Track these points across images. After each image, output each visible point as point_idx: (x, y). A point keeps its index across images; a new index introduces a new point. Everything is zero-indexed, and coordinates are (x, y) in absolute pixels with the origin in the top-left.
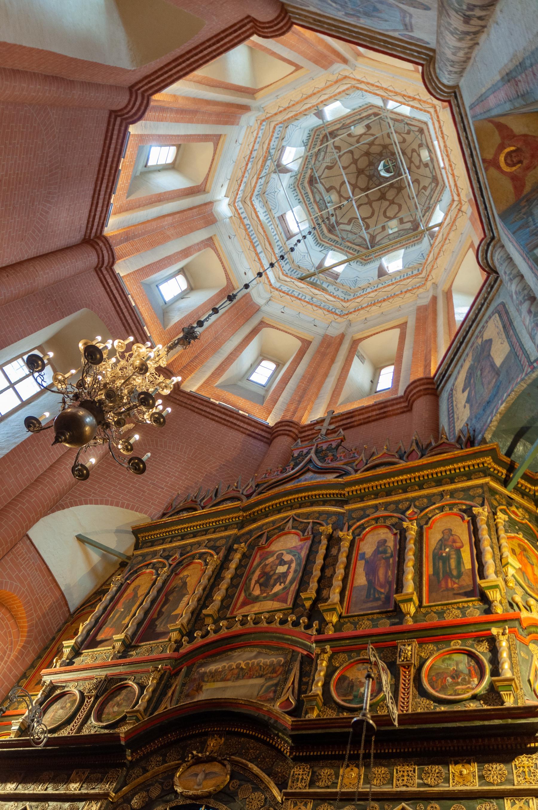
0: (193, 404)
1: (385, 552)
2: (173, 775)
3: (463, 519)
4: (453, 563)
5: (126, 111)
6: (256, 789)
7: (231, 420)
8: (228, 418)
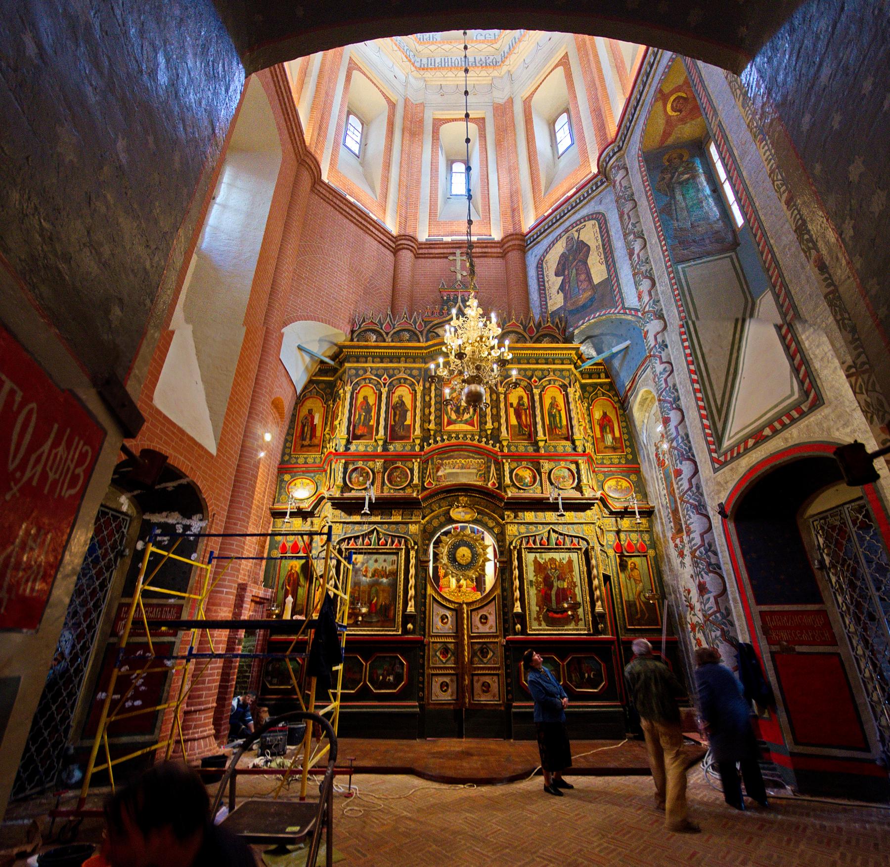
0: (335, 200)
1: (523, 405)
2: (449, 513)
4: (558, 418)
6: (490, 519)
7: (366, 224)
8: (363, 222)
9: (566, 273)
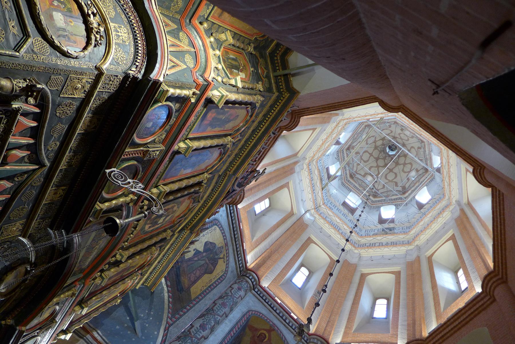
3: (120, 293)
5: (495, 284)
9: (204, 254)
